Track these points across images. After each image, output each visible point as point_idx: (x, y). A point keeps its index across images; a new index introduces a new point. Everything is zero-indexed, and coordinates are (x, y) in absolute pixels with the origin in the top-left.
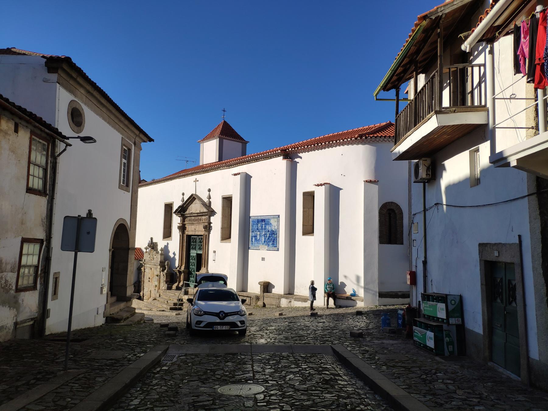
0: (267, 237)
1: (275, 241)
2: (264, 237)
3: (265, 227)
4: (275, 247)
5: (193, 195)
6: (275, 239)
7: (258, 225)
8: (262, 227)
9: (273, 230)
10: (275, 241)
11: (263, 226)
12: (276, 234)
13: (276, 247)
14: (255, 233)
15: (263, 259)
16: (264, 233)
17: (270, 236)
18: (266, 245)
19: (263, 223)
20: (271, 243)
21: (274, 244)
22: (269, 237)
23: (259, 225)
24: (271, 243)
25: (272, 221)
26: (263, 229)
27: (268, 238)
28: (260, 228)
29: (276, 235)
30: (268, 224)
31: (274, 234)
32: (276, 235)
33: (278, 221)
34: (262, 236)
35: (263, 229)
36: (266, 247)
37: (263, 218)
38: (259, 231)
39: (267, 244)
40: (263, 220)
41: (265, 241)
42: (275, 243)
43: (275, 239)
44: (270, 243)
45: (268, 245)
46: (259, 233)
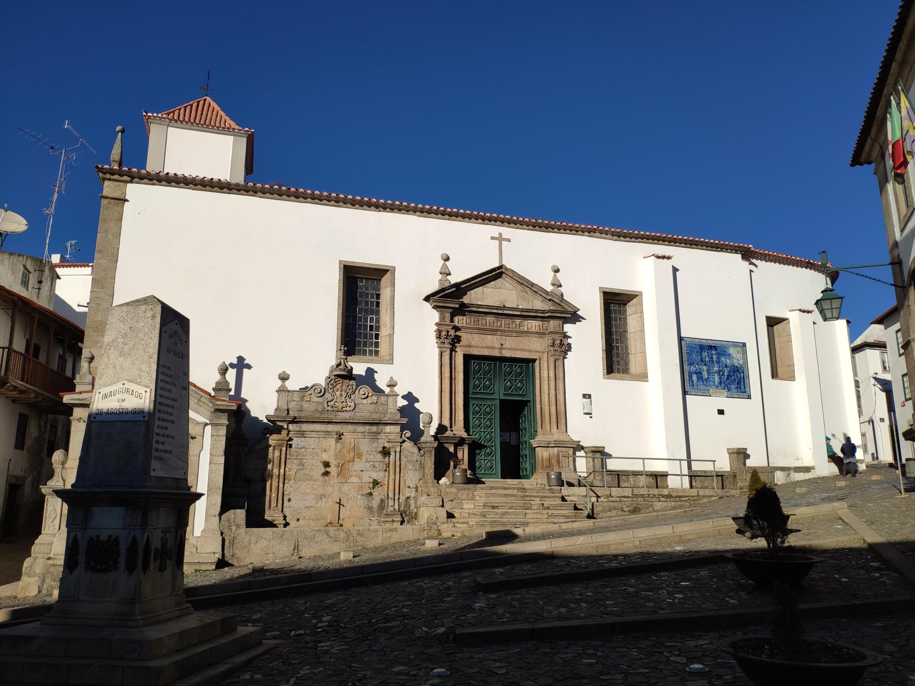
0: (723, 375)
1: (742, 383)
2: (719, 374)
3: (718, 358)
4: (742, 392)
5: (502, 268)
6: (742, 381)
7: (701, 353)
8: (712, 358)
9: (736, 365)
10: (742, 383)
11: (714, 356)
12: (743, 372)
13: (745, 392)
14: (697, 366)
15: (721, 412)
16: (716, 369)
17: (731, 374)
18: (724, 389)
19: (713, 352)
20: (733, 387)
21: (740, 388)
22: (729, 376)
23: (705, 354)
24: (733, 387)
25: (732, 351)
26: (715, 362)
27: (726, 377)
28: (707, 359)
29: (742, 374)
30: (725, 355)
31: (738, 371)
32: (742, 374)
33: (745, 353)
34: (713, 374)
35: (715, 362)
36: (725, 392)
37: (711, 343)
38: (705, 365)
39: (726, 388)
40: (711, 347)
41: (721, 383)
42: (742, 387)
43: (742, 381)
44: (731, 385)
45: (728, 388)
46: (705, 368)
